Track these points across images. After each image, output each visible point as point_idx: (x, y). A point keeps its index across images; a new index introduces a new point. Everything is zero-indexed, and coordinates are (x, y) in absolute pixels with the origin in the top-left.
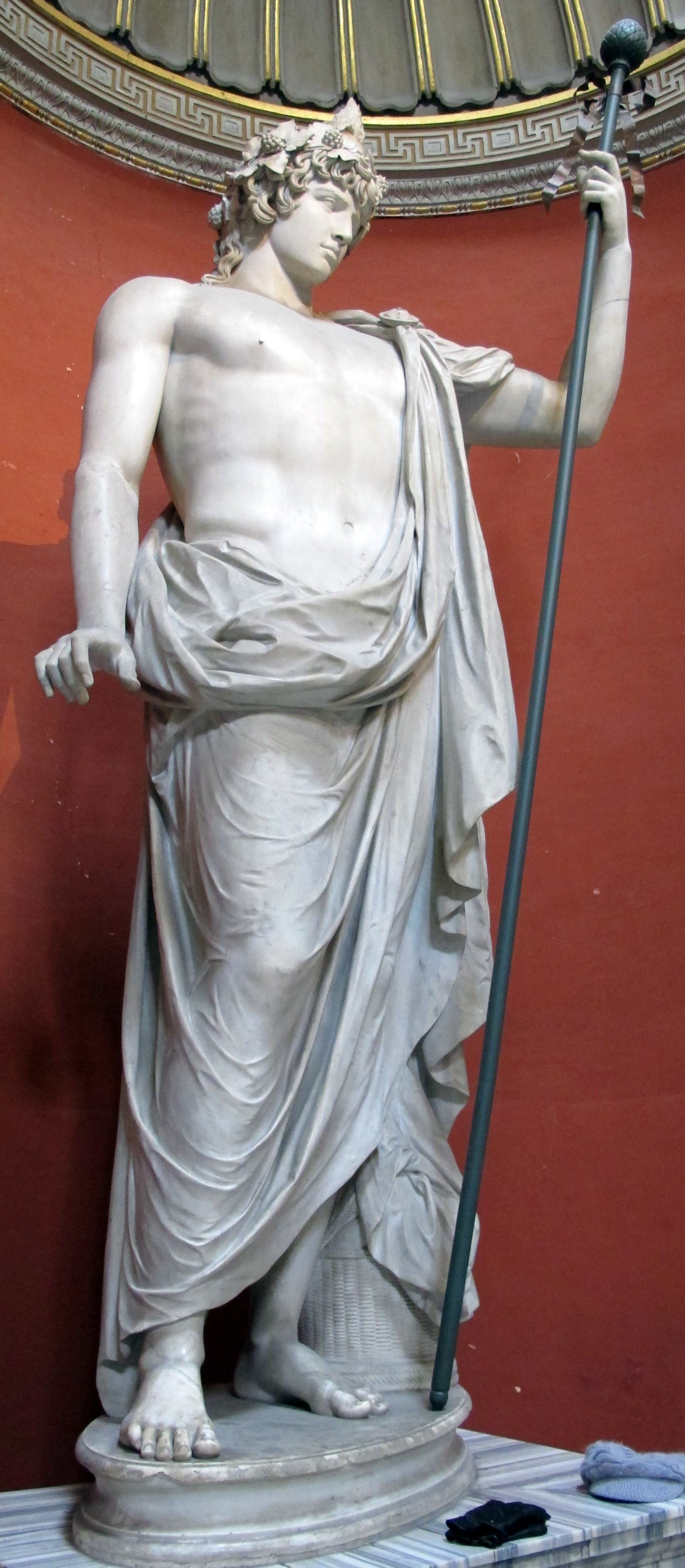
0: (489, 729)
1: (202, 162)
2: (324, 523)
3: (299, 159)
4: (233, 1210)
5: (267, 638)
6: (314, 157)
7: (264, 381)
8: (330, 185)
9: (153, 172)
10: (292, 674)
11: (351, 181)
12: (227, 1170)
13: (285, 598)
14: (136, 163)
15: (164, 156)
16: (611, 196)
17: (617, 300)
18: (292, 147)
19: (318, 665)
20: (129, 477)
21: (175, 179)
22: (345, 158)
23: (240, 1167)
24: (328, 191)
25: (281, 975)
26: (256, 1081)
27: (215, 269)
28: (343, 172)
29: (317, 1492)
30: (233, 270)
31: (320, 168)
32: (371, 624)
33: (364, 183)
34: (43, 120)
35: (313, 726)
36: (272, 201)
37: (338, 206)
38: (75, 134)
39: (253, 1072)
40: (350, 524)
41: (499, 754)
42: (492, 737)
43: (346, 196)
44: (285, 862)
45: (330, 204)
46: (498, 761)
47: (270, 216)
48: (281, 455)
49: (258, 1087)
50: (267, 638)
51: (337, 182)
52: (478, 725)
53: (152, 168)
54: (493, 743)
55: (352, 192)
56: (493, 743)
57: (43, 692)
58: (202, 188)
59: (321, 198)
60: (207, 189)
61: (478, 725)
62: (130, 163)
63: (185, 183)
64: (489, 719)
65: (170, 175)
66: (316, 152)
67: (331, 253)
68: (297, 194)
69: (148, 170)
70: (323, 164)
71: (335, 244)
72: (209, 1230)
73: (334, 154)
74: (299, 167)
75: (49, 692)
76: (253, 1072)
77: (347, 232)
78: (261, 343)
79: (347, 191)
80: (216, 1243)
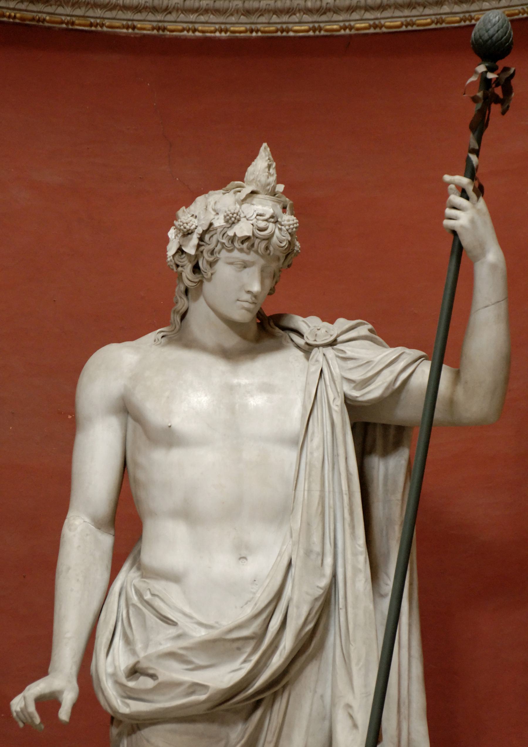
0: (348, 706)
1: (271, 10)
2: (222, 563)
3: (207, 237)
5: (153, 676)
6: (218, 233)
8: (236, 254)
9: (223, 34)
10: (173, 699)
13: (179, 637)
14: (203, 32)
15: (232, 15)
16: (462, 227)
18: (200, 230)
19: (191, 690)
20: (99, 525)
21: (248, 34)
22: (239, 234)
24: (233, 258)
27: (165, 323)
28: (242, 243)
30: (183, 316)
31: (224, 243)
32: (239, 649)
34: (99, 29)
35: (200, 727)
36: (196, 269)
37: (245, 265)
38: (134, 28)
40: (245, 558)
41: (355, 726)
42: (351, 713)
43: (251, 257)
45: (239, 266)
46: (355, 731)
48: (187, 514)
50: (153, 676)
51: (241, 250)
52: (342, 704)
53: (221, 31)
54: (351, 717)
55: (257, 252)
56: (351, 717)
57: (18, 726)
58: (279, 34)
60: (285, 34)
61: (342, 704)
62: (197, 34)
63: (260, 34)
64: (349, 699)
65: (240, 32)
66: (219, 230)
67: (246, 305)
69: (218, 34)
71: (247, 297)
73: (231, 233)
74: (209, 245)
75: (21, 725)
77: (256, 288)
78: (170, 426)
79: (252, 253)
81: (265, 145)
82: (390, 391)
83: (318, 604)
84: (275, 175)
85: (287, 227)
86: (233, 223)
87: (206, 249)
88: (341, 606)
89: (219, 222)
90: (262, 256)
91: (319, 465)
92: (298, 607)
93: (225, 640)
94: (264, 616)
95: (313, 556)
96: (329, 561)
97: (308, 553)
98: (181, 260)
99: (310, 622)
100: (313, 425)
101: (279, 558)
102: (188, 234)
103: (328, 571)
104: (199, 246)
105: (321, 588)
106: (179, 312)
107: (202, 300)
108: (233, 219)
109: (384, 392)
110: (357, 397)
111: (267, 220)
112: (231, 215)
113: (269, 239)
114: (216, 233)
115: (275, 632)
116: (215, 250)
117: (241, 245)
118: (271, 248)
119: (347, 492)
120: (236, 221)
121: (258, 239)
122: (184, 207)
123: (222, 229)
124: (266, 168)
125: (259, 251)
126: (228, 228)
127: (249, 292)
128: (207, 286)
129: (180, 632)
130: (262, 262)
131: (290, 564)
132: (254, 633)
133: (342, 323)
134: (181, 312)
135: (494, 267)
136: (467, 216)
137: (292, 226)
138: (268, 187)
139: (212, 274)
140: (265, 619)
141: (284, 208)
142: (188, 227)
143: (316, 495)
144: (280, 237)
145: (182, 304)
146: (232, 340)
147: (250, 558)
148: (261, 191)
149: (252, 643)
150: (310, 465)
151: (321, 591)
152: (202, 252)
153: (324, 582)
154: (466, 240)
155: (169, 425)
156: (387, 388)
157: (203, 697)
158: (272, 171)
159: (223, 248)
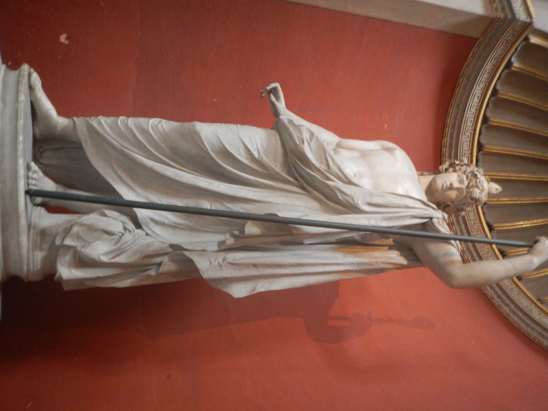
4: (112, 129)
8: (465, 177)
11: (471, 180)
12: (126, 121)
23: (126, 125)
25: (194, 126)
26: (156, 127)
29: (10, 98)
36: (446, 170)
37: (461, 182)
39: (160, 125)
43: (466, 182)
44: (231, 130)
49: (155, 128)
51: (467, 177)
55: (469, 183)
59: (459, 176)
67: (445, 185)
68: (455, 171)
70: (468, 171)
71: (448, 185)
72: (104, 120)
76: (160, 125)
80: (100, 123)
93: (326, 154)
94: (340, 174)
97: (371, 195)
99: (342, 197)
113: (477, 186)
118: (472, 189)
127: (451, 184)
135: (532, 262)
149: (326, 168)
151: (356, 201)
157: (297, 142)
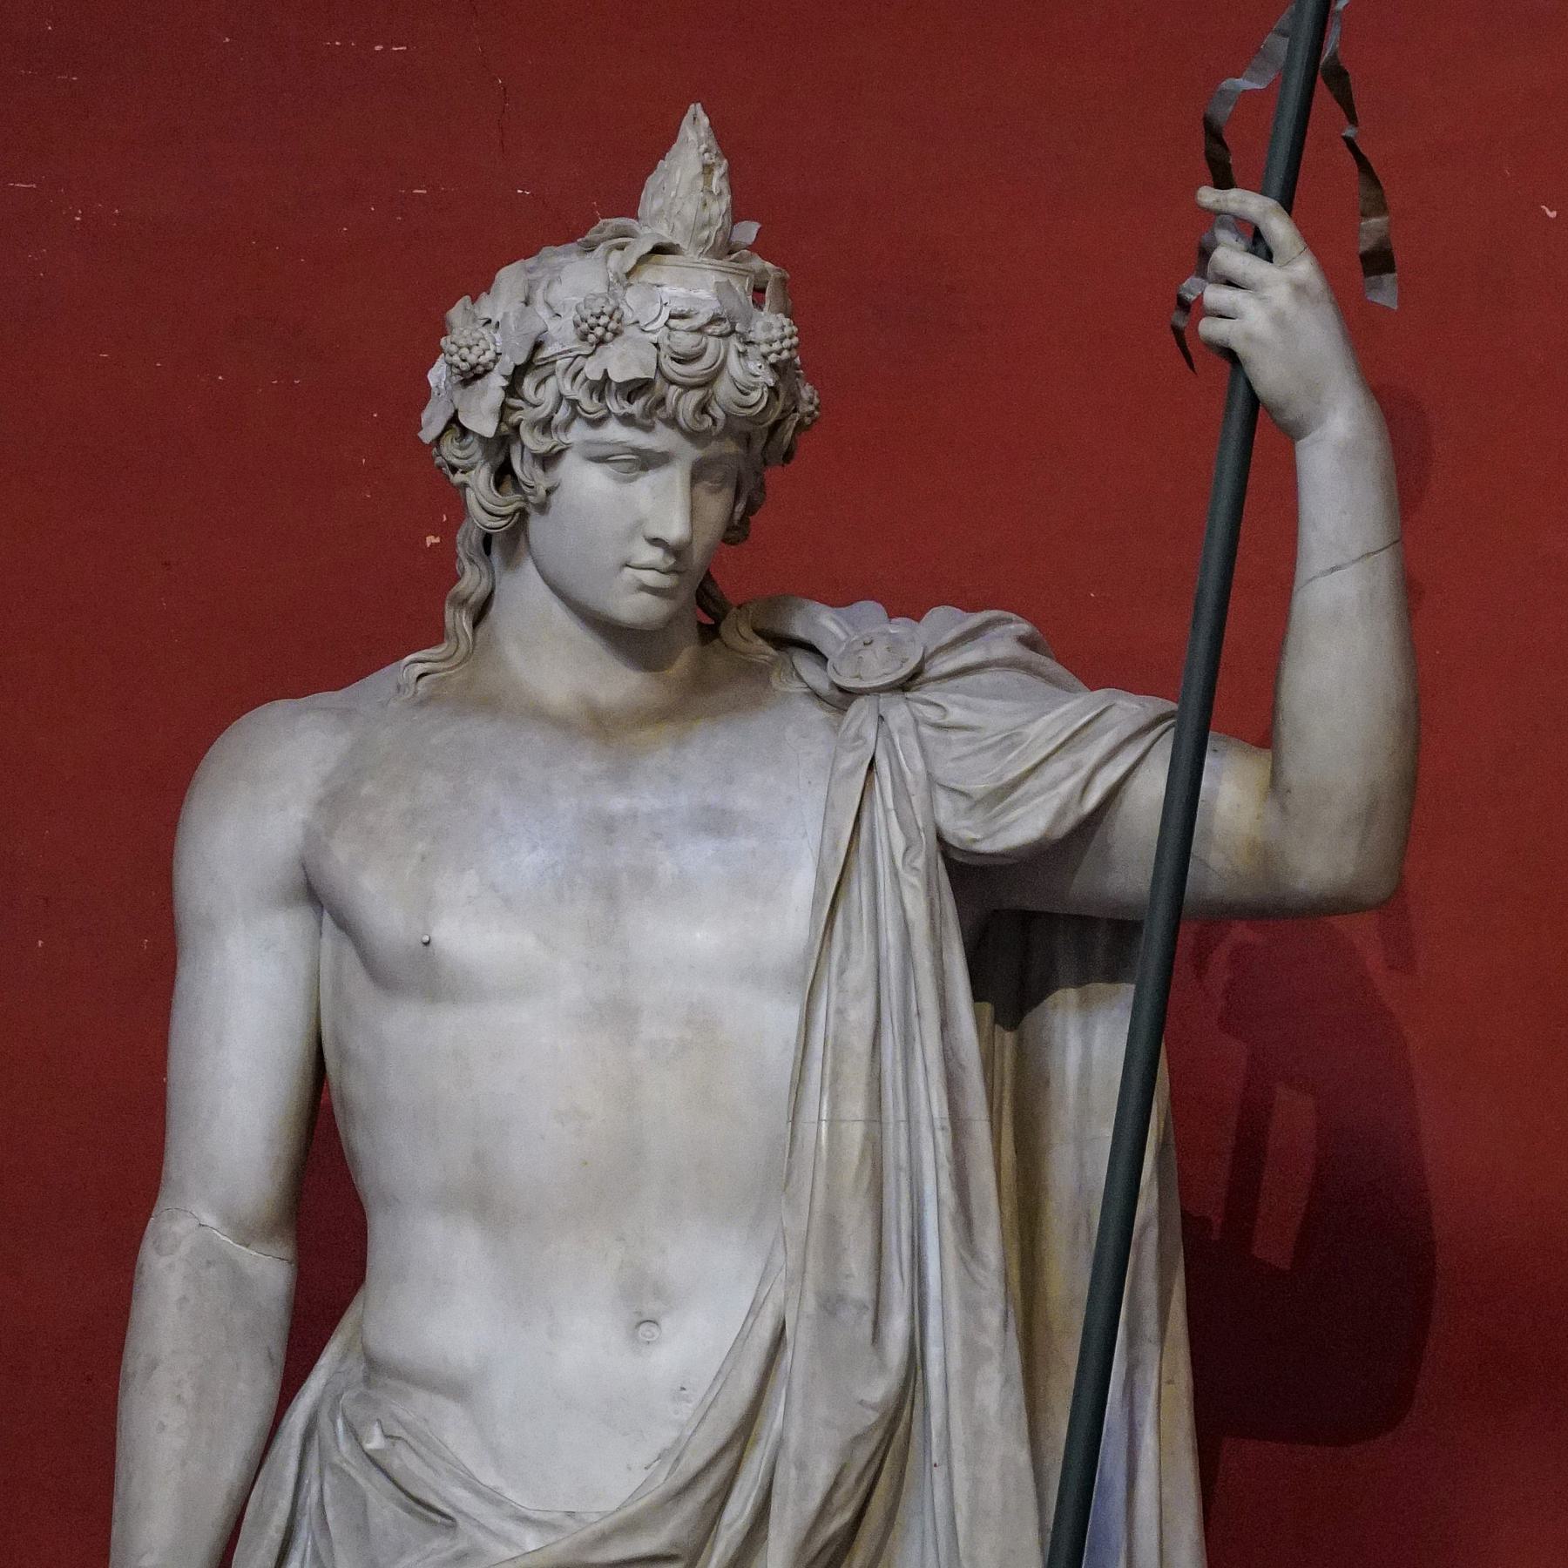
2: (586, 1341)
3: (528, 384)
6: (559, 374)
7: (447, 1026)
17: (1333, 570)
18: (507, 364)
30: (481, 612)
33: (695, 396)
37: (647, 461)
43: (661, 439)
45: (626, 466)
47: (503, 517)
48: (483, 1201)
51: (627, 420)
55: (672, 422)
66: (561, 363)
67: (650, 578)
71: (654, 555)
73: (593, 371)
78: (427, 944)
79: (659, 426)
81: (696, 109)
82: (1069, 822)
83: (863, 1454)
84: (727, 198)
85: (765, 348)
86: (601, 341)
87: (525, 416)
88: (935, 1459)
89: (562, 337)
90: (692, 436)
91: (860, 1043)
92: (801, 1466)
94: (703, 1492)
95: (847, 1314)
96: (898, 1325)
97: (831, 1304)
98: (459, 453)
99: (842, 1508)
100: (847, 927)
101: (750, 1321)
102: (472, 376)
103: (895, 1351)
104: (504, 410)
105: (873, 1407)
106: (466, 601)
107: (529, 568)
108: (599, 331)
109: (1050, 829)
110: (975, 841)
111: (700, 330)
112: (592, 321)
113: (708, 382)
114: (553, 374)
115: (739, 1539)
116: (554, 422)
117: (625, 404)
119: (947, 1124)
120: (609, 335)
121: (673, 387)
122: (467, 297)
123: (569, 360)
124: (696, 177)
125: (681, 419)
126: (587, 356)
127: (655, 542)
128: (537, 526)
129: (462, 1545)
130: (690, 453)
131: (779, 1339)
132: (674, 1544)
133: (944, 622)
134: (473, 600)
136: (1271, 306)
137: (776, 346)
138: (706, 233)
139: (549, 492)
140: (709, 1501)
141: (758, 292)
142: (472, 358)
143: (855, 1133)
144: (746, 376)
145: (471, 581)
146: (619, 684)
147: (666, 1323)
148: (684, 246)
150: (837, 1048)
151: (873, 1416)
152: (516, 428)
153: (880, 1390)
154: (1269, 376)
155: (426, 939)
156: (1061, 813)
158: (718, 182)
159: (575, 415)
